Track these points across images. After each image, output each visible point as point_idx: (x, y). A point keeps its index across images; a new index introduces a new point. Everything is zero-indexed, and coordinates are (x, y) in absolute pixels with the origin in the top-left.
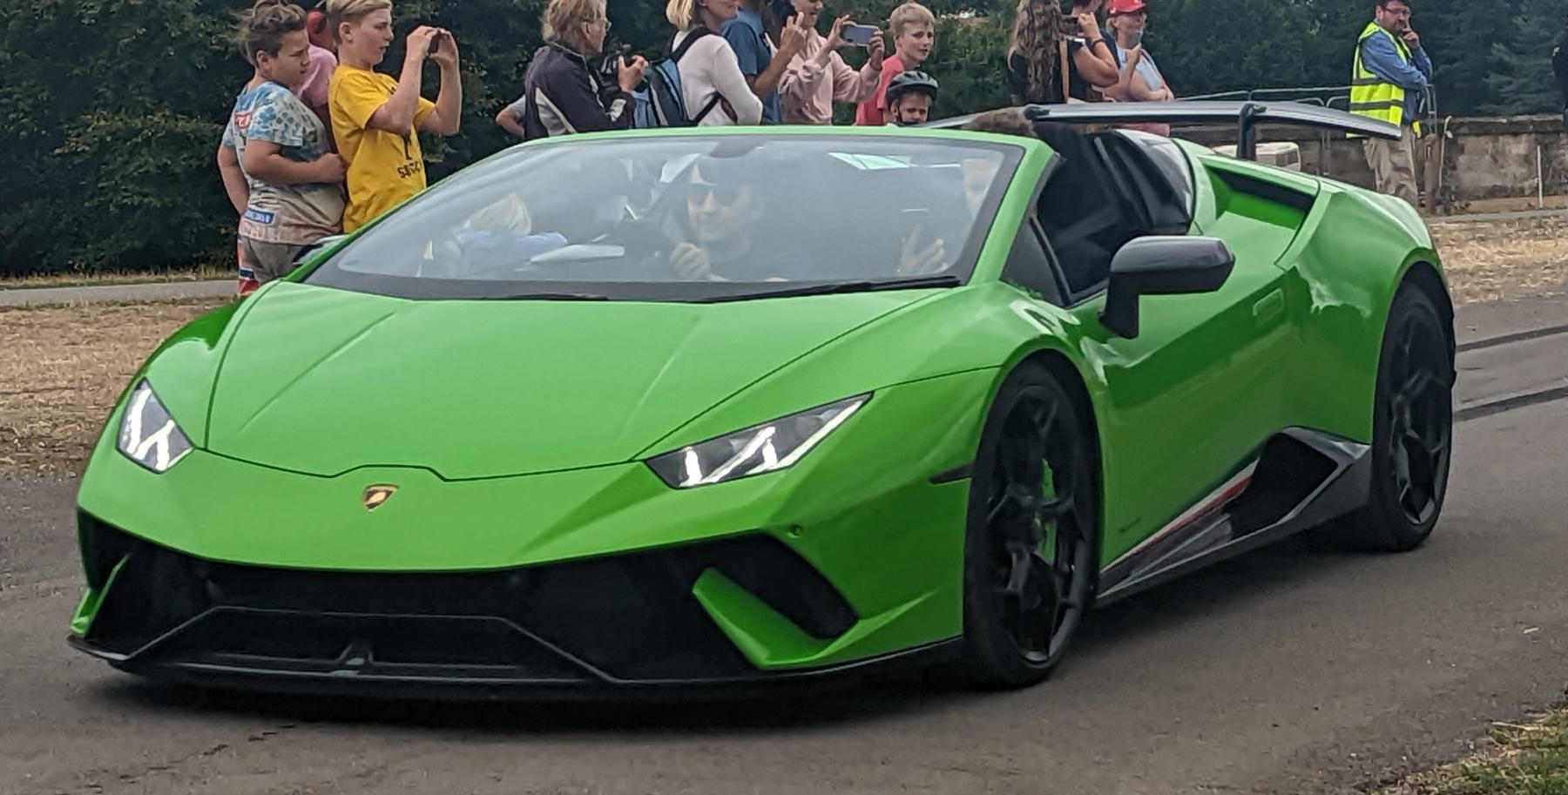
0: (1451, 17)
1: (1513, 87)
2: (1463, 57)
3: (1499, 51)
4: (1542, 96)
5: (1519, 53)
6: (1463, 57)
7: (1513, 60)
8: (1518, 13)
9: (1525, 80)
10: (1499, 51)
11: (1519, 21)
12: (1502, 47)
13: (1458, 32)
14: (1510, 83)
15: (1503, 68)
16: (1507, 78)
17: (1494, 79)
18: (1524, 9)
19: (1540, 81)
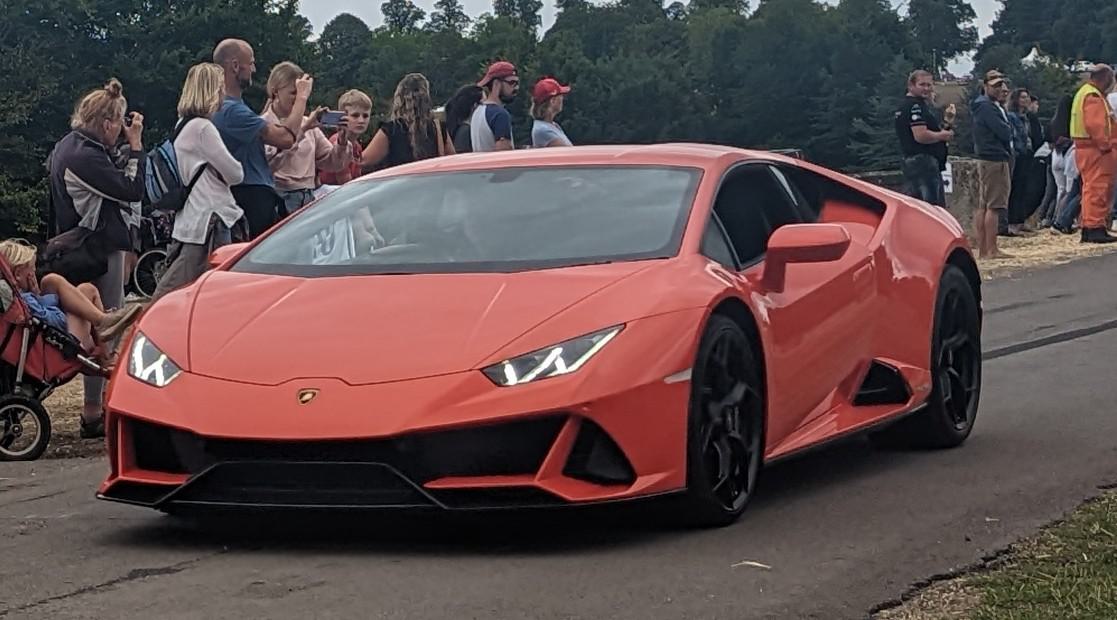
0: (821, 99)
1: (871, 152)
2: (829, 130)
3: (858, 123)
4: (893, 159)
5: (873, 125)
6: (829, 130)
7: (869, 130)
8: (874, 94)
9: (880, 146)
10: (858, 123)
11: (875, 101)
12: (860, 120)
13: (826, 110)
14: (867, 149)
15: (861, 137)
16: (866, 145)
17: (854, 146)
18: (877, 91)
19: (890, 146)
